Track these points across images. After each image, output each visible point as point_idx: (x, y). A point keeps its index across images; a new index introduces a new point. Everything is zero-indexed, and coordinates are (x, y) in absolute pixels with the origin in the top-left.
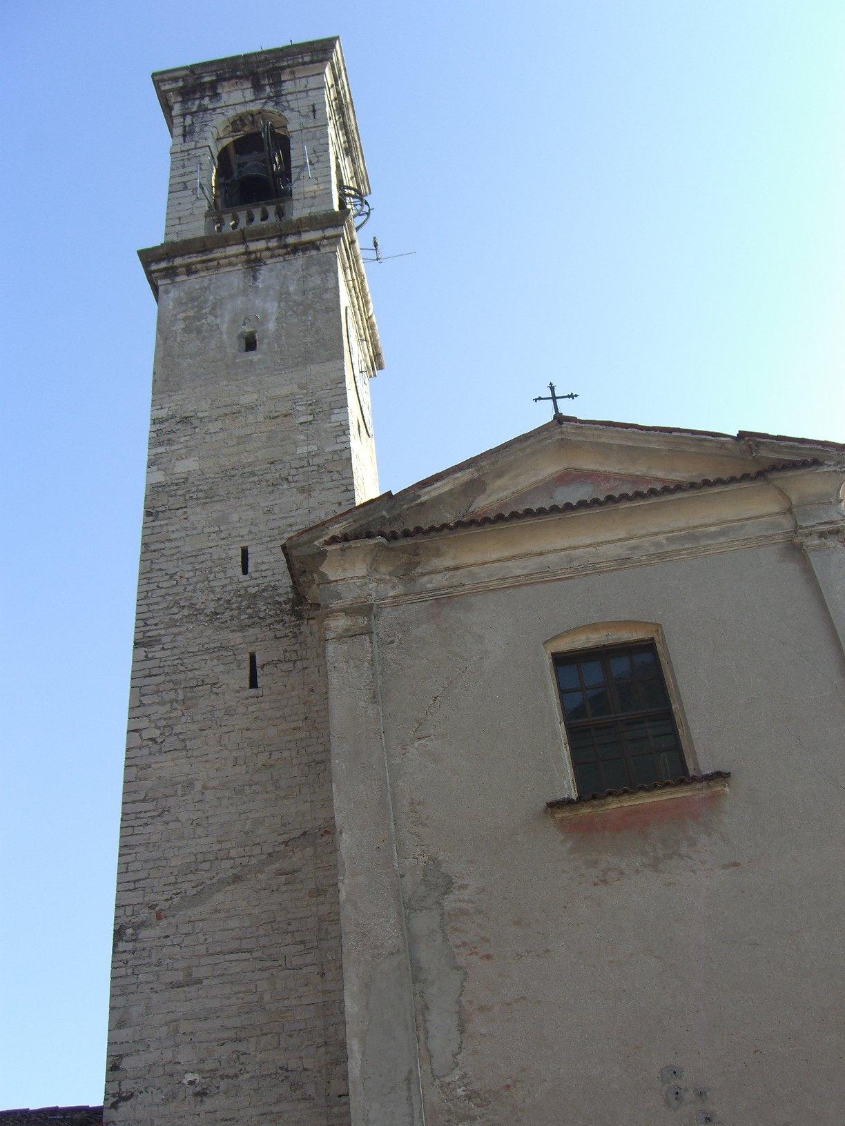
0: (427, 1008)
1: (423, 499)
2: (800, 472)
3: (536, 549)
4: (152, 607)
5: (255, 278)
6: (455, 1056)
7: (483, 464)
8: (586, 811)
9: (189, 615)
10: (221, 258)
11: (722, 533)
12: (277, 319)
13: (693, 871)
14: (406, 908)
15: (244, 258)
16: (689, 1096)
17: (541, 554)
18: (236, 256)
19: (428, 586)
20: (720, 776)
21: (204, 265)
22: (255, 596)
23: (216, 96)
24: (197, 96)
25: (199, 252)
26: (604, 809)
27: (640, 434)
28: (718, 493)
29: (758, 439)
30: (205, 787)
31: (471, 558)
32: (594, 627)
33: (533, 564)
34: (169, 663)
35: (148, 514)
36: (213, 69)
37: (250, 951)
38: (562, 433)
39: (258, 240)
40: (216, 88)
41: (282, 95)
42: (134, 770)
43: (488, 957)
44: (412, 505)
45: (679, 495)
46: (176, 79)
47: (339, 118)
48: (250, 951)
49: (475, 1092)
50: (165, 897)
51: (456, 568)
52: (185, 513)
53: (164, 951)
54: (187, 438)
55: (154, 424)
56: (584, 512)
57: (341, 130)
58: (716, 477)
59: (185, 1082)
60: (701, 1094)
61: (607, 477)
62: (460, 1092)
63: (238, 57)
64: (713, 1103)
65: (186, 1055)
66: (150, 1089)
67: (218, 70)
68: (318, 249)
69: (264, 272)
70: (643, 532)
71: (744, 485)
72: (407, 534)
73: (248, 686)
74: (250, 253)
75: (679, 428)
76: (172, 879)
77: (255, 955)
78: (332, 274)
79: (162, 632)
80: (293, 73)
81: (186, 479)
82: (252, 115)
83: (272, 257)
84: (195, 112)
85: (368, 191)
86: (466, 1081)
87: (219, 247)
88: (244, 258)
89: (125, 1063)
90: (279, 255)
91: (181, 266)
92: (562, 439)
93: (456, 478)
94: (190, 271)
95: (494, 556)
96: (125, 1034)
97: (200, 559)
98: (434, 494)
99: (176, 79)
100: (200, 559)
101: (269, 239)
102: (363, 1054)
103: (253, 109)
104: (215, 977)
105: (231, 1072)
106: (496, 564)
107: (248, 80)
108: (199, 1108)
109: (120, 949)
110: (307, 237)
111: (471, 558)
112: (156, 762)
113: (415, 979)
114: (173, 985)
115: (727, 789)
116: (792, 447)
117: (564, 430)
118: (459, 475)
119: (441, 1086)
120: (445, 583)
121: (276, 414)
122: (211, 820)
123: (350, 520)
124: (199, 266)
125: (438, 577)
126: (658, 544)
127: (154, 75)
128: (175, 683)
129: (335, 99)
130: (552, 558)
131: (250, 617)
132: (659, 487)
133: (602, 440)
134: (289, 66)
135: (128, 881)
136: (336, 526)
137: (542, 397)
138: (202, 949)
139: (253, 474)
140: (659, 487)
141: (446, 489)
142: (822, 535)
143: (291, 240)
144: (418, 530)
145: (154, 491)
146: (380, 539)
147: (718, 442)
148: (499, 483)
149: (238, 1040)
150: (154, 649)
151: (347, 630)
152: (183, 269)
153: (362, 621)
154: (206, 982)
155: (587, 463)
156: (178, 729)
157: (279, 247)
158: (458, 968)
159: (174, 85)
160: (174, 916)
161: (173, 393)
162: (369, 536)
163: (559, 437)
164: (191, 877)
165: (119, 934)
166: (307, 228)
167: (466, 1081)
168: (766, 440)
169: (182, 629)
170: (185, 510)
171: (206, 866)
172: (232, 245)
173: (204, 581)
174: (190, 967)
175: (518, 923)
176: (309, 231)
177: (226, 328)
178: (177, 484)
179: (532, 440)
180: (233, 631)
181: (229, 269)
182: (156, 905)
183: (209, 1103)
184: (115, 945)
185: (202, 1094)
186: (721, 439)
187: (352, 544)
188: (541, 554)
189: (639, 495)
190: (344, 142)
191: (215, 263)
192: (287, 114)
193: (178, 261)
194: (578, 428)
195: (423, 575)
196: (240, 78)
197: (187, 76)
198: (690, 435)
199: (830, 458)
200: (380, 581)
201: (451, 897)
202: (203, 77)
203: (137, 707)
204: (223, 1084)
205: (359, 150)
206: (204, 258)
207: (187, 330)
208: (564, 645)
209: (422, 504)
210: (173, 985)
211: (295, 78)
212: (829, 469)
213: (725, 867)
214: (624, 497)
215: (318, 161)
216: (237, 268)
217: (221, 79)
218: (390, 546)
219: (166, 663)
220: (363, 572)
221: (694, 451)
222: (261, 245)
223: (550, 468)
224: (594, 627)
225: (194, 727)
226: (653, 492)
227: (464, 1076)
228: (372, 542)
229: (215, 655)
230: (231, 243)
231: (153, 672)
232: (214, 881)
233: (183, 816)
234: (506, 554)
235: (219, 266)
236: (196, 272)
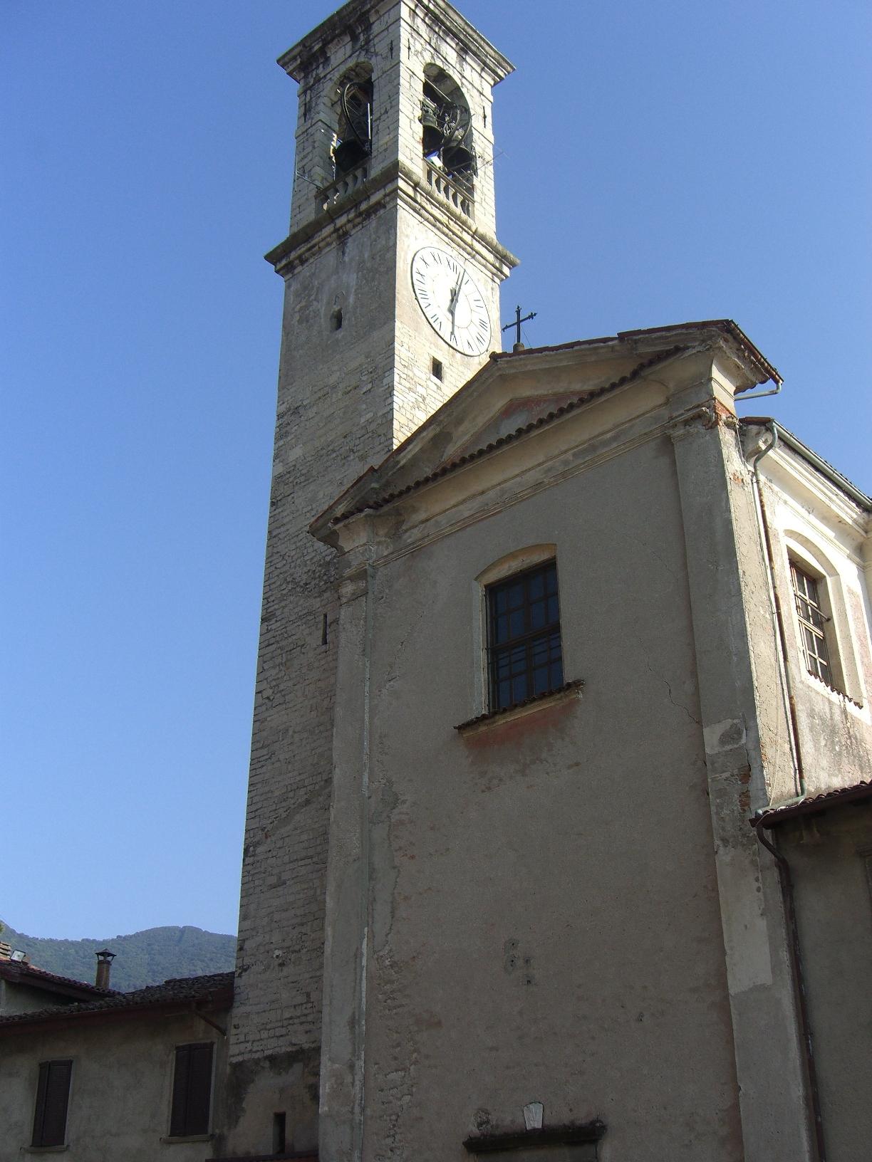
0: (375, 899)
1: (402, 463)
2: (670, 361)
3: (480, 488)
4: (272, 587)
5: (344, 253)
6: (387, 935)
7: (441, 418)
8: (502, 721)
9: (292, 588)
10: (319, 242)
11: (615, 438)
12: (355, 291)
13: (547, 773)
14: (370, 823)
15: (335, 235)
16: (520, 963)
17: (483, 492)
18: (329, 236)
19: (408, 541)
20: (577, 684)
21: (311, 252)
22: (329, 563)
23: (327, 59)
24: (314, 67)
25: (304, 242)
26: (494, 725)
27: (551, 356)
28: (605, 401)
29: (635, 337)
30: (294, 732)
31: (437, 508)
32: (512, 556)
33: (475, 504)
34: (279, 632)
35: (273, 504)
36: (318, 36)
37: (311, 857)
38: (499, 369)
39: (342, 215)
40: (326, 53)
41: (371, 41)
42: (258, 723)
43: (413, 857)
44: (395, 470)
45: (574, 413)
46: (294, 58)
47: (440, 28)
48: (311, 857)
49: (395, 962)
50: (270, 821)
51: (427, 520)
52: (293, 498)
53: (268, 861)
54: (296, 428)
55: (278, 419)
56: (505, 448)
57: (448, 35)
58: (619, 378)
59: (275, 956)
60: (527, 961)
61: (537, 401)
62: (387, 963)
63: (333, 17)
64: (534, 969)
65: (276, 938)
66: (258, 962)
67: (321, 36)
68: (385, 207)
69: (351, 245)
70: (557, 452)
71: (626, 387)
72: (386, 501)
73: (321, 644)
74: (338, 230)
75: (579, 341)
76: (274, 807)
77: (314, 860)
78: (393, 230)
79: (276, 607)
80: (377, 12)
81: (295, 466)
82: (352, 70)
83: (354, 227)
84: (313, 85)
85: (509, 69)
86: (391, 954)
87: (317, 232)
88: (335, 235)
89: (247, 945)
90: (359, 224)
91: (295, 259)
92: (501, 375)
93: (424, 437)
94: (302, 261)
95: (453, 502)
96: (248, 924)
97: (300, 537)
98: (409, 456)
99: (294, 58)
100: (300, 537)
101: (348, 211)
102: (333, 937)
103: (351, 65)
104: (293, 879)
105: (297, 948)
106: (454, 510)
107: (346, 34)
108: (281, 974)
109: (246, 863)
110: (375, 198)
111: (437, 508)
112: (270, 716)
113: (371, 878)
114: (273, 887)
115: (581, 696)
116: (662, 337)
117: (499, 366)
118: (424, 434)
119: (377, 959)
120: (419, 535)
121: (349, 389)
122: (296, 758)
123: (348, 499)
124: (307, 255)
125: (415, 531)
126: (566, 463)
127: (278, 61)
128: (281, 648)
129: (426, 15)
130: (491, 494)
131: (326, 583)
132: (575, 400)
133: (530, 368)
134: (373, 7)
135: (253, 813)
136: (340, 507)
137: (508, 325)
138: (286, 859)
139: (334, 451)
140: (575, 400)
141: (417, 449)
142: (687, 423)
143: (364, 207)
144: (392, 496)
145: (278, 480)
146: (367, 511)
147: (608, 346)
148: (461, 428)
149: (302, 925)
150: (271, 623)
151: (353, 594)
152: (297, 262)
153: (362, 584)
154: (288, 883)
155: (527, 390)
156: (282, 687)
157: (356, 217)
158: (394, 868)
159: (295, 65)
160: (274, 835)
161: (290, 387)
162: (360, 510)
163: (498, 374)
164: (284, 804)
165: (246, 851)
166: (373, 191)
167: (391, 954)
168: (640, 336)
169: (287, 602)
170: (292, 495)
171: (291, 794)
172: (325, 227)
173: (301, 557)
174: (280, 873)
175: (432, 829)
176: (375, 192)
177: (323, 309)
178: (289, 473)
179: (476, 384)
180: (316, 597)
181: (328, 249)
182: (265, 828)
183: (286, 971)
184: (244, 860)
185: (282, 965)
186: (610, 343)
187: (351, 520)
188: (483, 492)
189: (562, 411)
190: (457, 44)
191: (317, 247)
192: (373, 61)
193: (293, 255)
194: (508, 362)
195: (406, 531)
196: (339, 35)
197: (301, 51)
198: (587, 346)
199: (694, 339)
200: (379, 543)
201: (396, 811)
202: (313, 47)
203: (261, 671)
204: (293, 956)
205: (479, 40)
206: (309, 246)
207: (300, 322)
208: (492, 577)
209: (403, 467)
210: (273, 887)
211: (380, 16)
212: (694, 351)
213: (570, 767)
214: (551, 416)
215: (391, 107)
216: (333, 246)
217: (326, 44)
218: (378, 513)
219: (277, 633)
220: (363, 541)
221: (593, 359)
222: (343, 220)
223: (499, 403)
224: (512, 556)
225: (290, 684)
226: (582, 401)
227: (391, 950)
228: (363, 515)
229: (304, 621)
230: (325, 225)
231: (271, 642)
232: (296, 806)
233: (282, 757)
234: (460, 498)
235: (320, 249)
236: (307, 260)
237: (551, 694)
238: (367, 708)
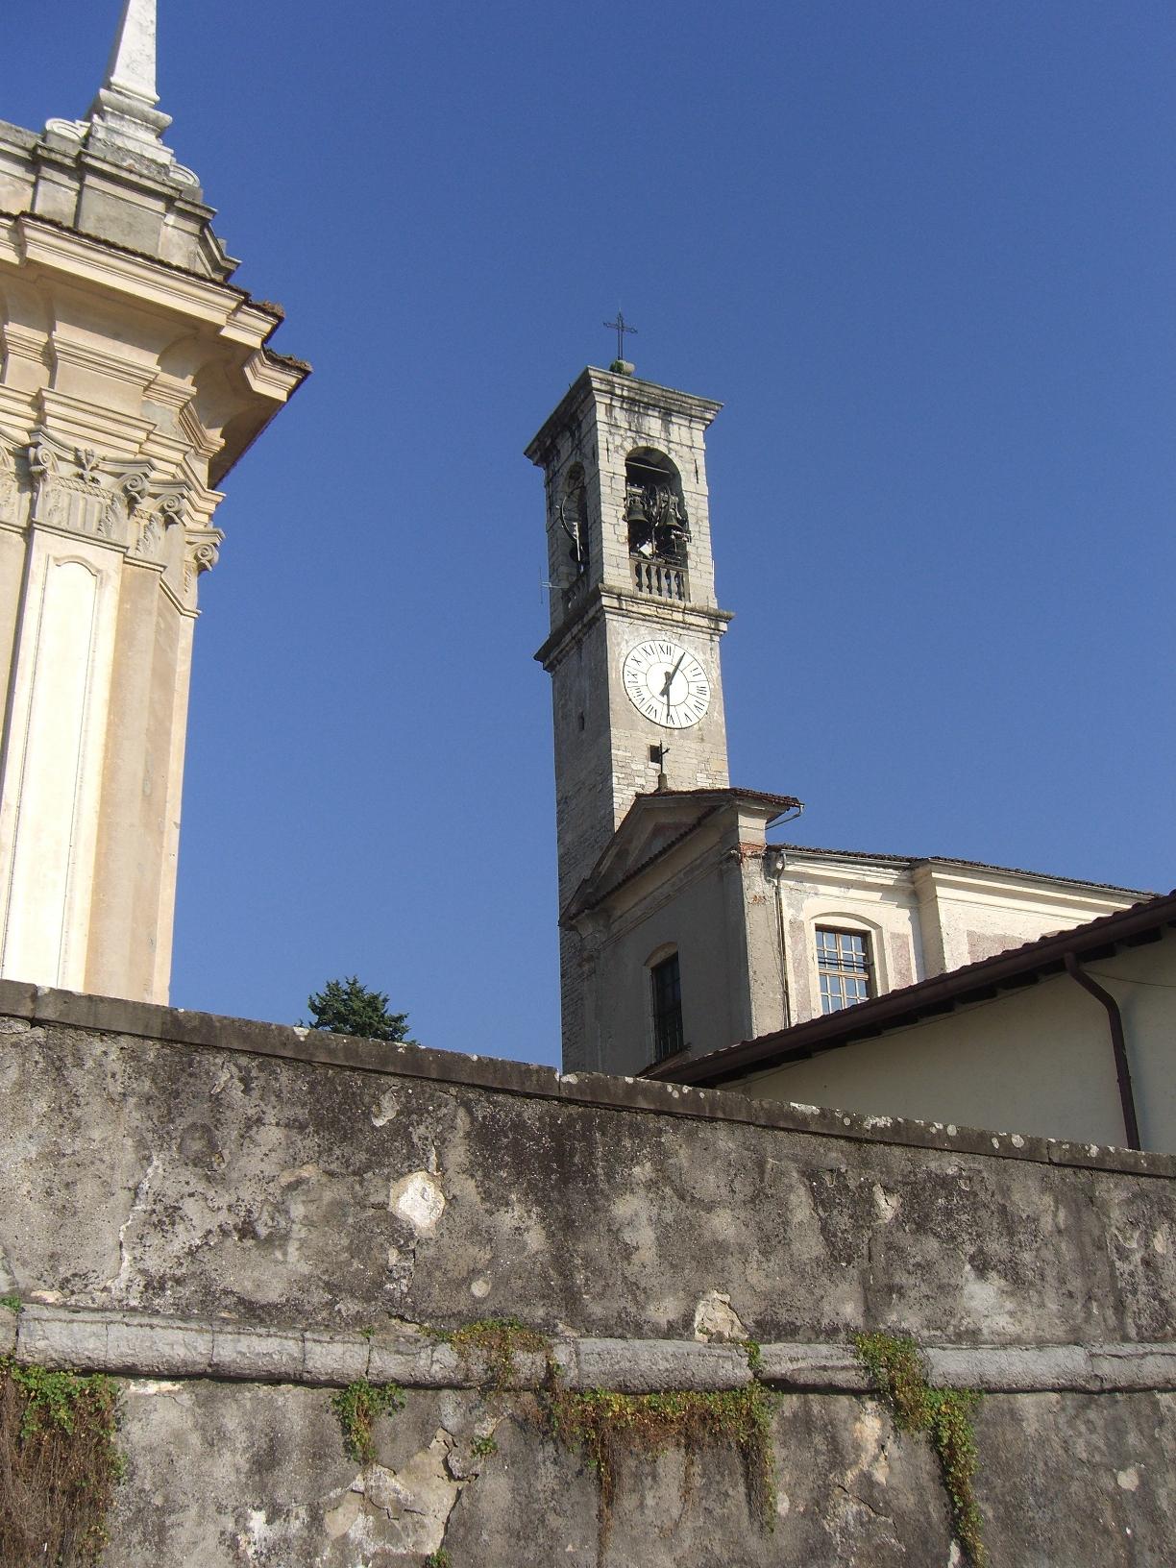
1: (603, 872)
15: (574, 641)
18: (570, 642)
57: (648, 409)
80: (582, 412)
88: (574, 641)
95: (632, 903)
127: (529, 453)
128: (572, 999)
143: (585, 620)
152: (555, 662)
155: (665, 819)
190: (660, 412)
205: (680, 398)
208: (654, 962)
235: (568, 652)
237: (675, 1054)
238: (600, 1057)
